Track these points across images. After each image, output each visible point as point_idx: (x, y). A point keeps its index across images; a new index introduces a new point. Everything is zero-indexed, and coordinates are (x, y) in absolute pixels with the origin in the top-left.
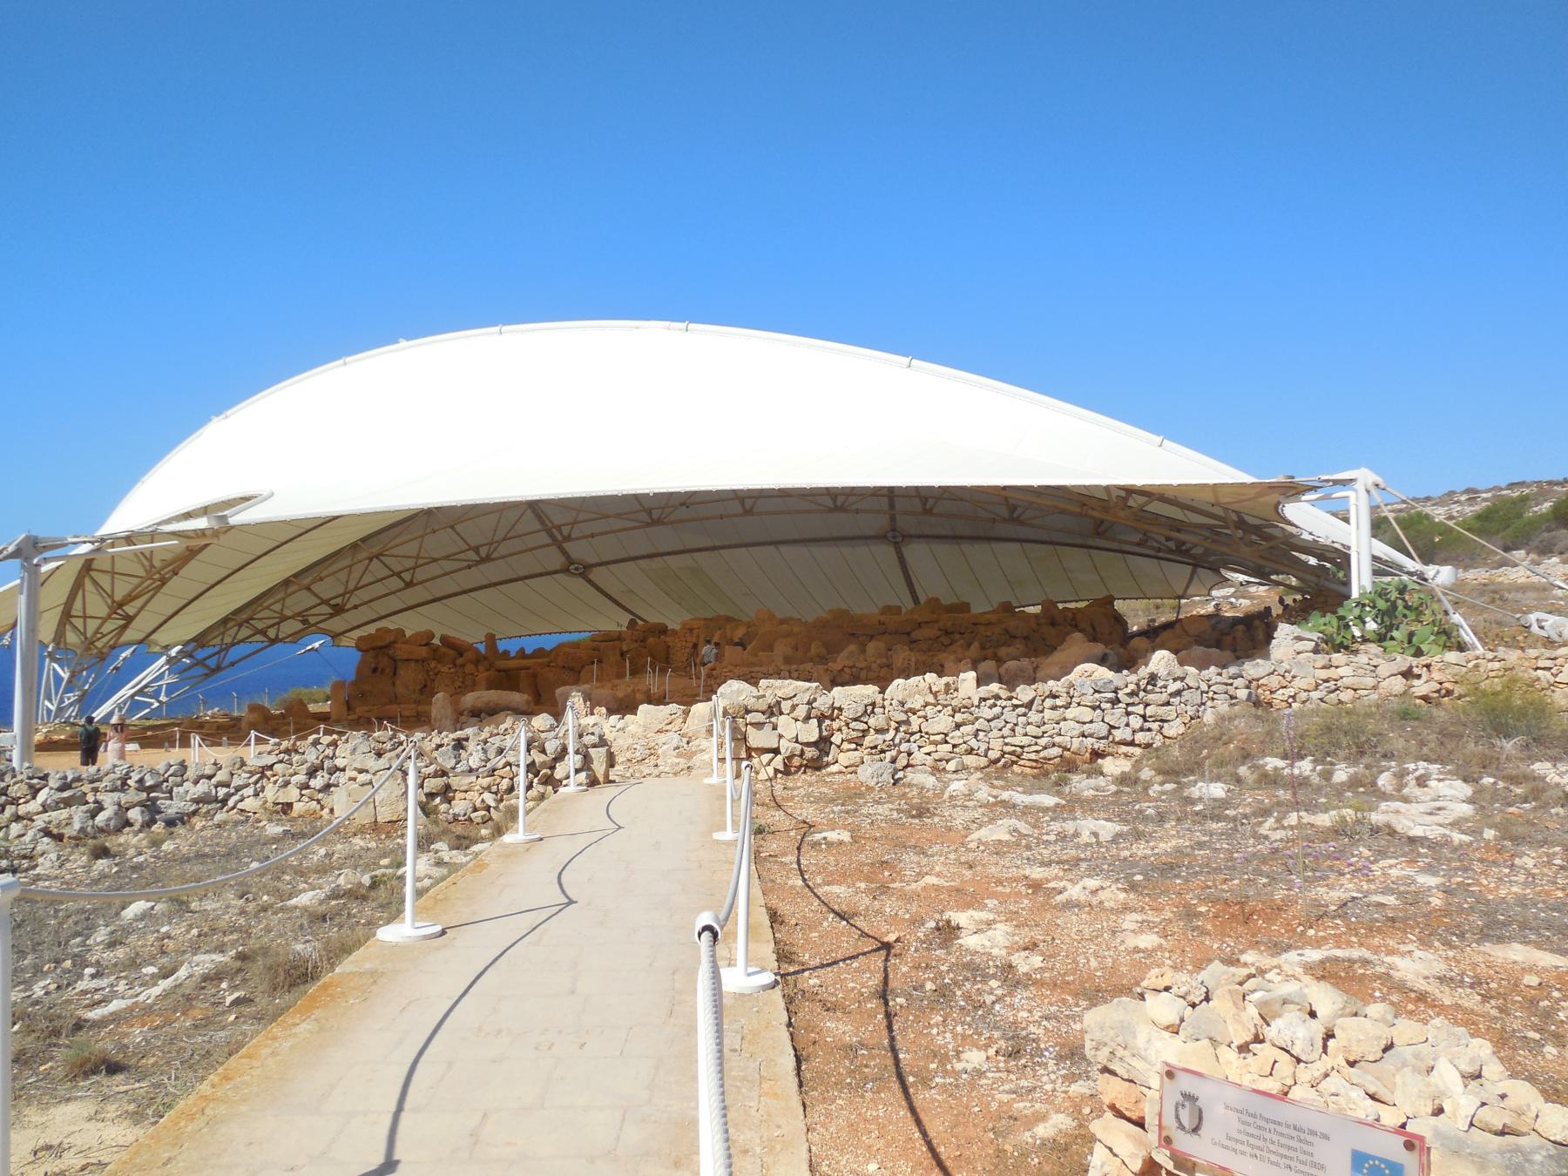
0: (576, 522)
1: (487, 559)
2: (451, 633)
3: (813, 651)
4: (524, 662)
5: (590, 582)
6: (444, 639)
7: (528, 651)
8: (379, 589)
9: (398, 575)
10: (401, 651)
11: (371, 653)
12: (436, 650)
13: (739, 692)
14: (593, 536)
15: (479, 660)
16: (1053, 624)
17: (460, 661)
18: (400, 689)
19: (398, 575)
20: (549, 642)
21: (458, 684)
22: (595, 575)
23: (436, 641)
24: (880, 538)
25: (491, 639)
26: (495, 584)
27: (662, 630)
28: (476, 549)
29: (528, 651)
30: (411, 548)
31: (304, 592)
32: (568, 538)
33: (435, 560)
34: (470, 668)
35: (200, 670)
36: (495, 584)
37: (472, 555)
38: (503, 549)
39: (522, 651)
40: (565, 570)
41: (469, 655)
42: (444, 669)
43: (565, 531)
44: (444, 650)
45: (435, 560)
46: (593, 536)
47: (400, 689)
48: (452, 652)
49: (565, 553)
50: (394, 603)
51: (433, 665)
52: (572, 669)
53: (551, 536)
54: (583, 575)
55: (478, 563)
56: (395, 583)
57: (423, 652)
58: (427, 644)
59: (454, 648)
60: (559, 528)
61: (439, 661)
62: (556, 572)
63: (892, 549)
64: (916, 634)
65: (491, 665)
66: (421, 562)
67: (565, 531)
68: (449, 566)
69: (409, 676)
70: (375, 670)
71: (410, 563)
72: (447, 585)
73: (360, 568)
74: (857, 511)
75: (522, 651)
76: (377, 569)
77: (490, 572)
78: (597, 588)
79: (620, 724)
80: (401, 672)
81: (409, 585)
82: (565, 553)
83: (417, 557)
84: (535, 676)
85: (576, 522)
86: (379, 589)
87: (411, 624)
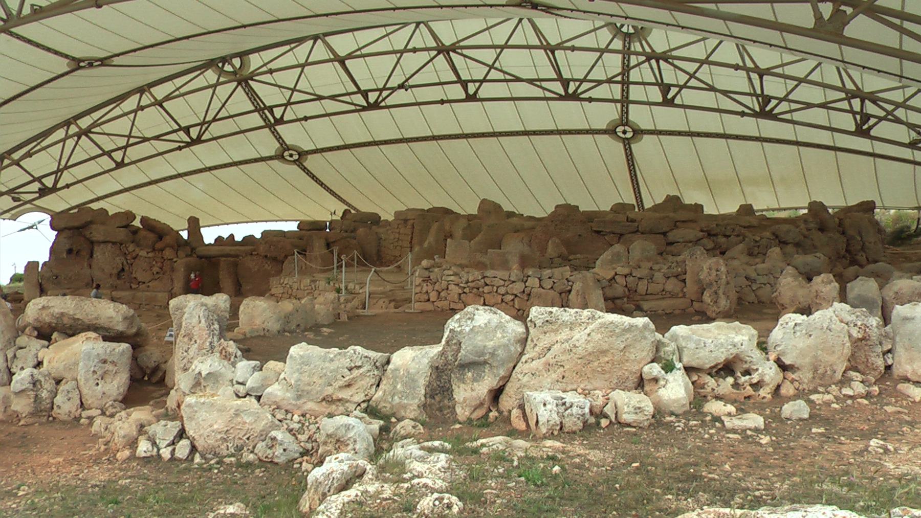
0: (289, 103)
1: (198, 141)
2: (154, 215)
3: (551, 250)
4: (227, 249)
5: (304, 169)
6: (144, 220)
7: (238, 238)
8: (92, 168)
9: (109, 154)
11: (64, 235)
12: (136, 231)
13: (487, 330)
14: (306, 119)
15: (180, 244)
16: (822, 229)
19: (109, 154)
20: (256, 230)
21: (156, 269)
22: (311, 162)
23: (137, 223)
24: (611, 131)
25: (194, 225)
26: (210, 169)
27: (374, 219)
28: (187, 130)
29: (238, 238)
30: (122, 127)
31: (15, 167)
32: (280, 121)
33: (145, 140)
34: (168, 253)
36: (210, 169)
37: (182, 136)
38: (216, 129)
39: (232, 236)
40: (280, 157)
41: (168, 239)
42: (143, 253)
43: (278, 112)
44: (143, 233)
45: (145, 140)
46: (306, 119)
47: (97, 274)
48: (151, 236)
49: (279, 138)
50: (107, 185)
51: (131, 248)
52: (275, 259)
53: (265, 119)
54: (299, 163)
55: (188, 145)
57: (122, 235)
58: (126, 227)
59: (156, 233)
60: (271, 109)
62: (271, 158)
63: (621, 145)
64: (671, 236)
65: (193, 249)
66: (132, 141)
67: (278, 112)
68: (162, 146)
70: (70, 251)
71: (122, 142)
72: (159, 169)
73: (70, 143)
74: (590, 100)
75: (232, 236)
76: (86, 147)
77: (206, 155)
78: (313, 177)
79: (253, 381)
80: (98, 254)
81: (120, 165)
82: (279, 138)
83: (129, 136)
84: (236, 265)
85: (289, 103)
86: (92, 168)
87: (113, 206)
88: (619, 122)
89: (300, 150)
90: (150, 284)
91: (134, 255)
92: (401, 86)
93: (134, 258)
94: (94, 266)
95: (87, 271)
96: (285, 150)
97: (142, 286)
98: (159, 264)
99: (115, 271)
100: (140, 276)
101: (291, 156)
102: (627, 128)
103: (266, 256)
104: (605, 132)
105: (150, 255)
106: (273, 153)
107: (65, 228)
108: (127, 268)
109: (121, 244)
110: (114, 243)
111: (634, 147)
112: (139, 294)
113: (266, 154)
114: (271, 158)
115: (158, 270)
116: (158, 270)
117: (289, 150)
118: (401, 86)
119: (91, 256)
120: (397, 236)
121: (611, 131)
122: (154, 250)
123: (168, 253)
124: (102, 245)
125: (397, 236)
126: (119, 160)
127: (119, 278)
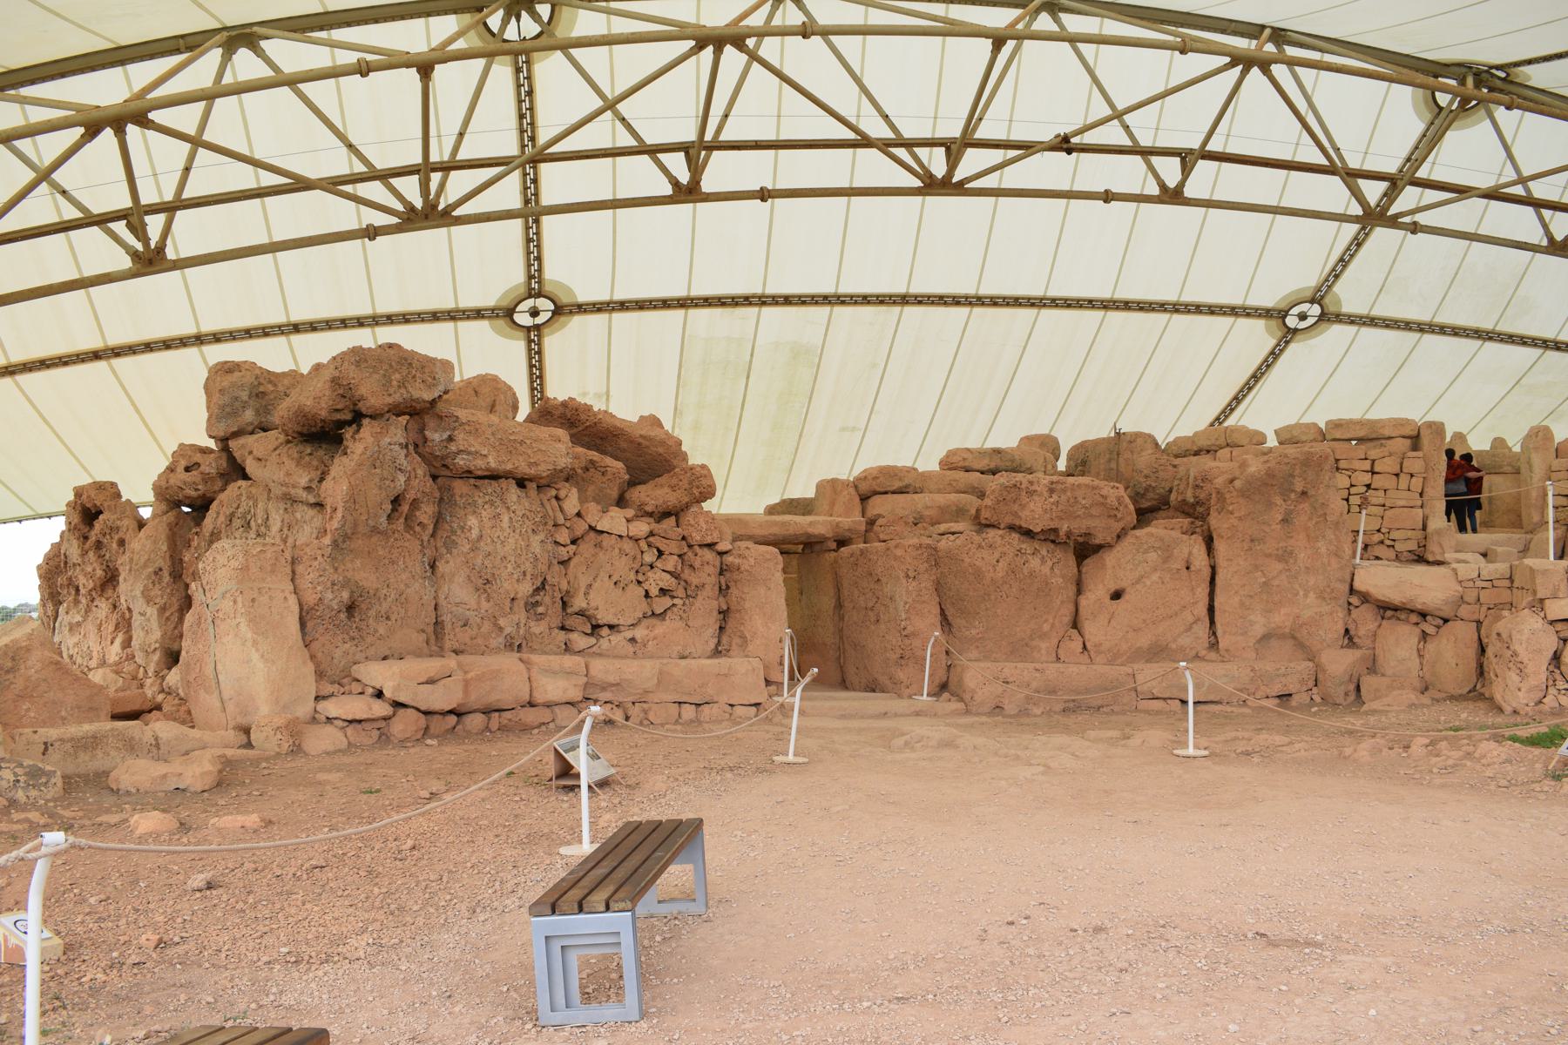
18: (458, 592)
21: (657, 579)
42: (614, 521)
47: (458, 592)
56: (100, 251)
62: (478, 314)
88: (1309, 294)
90: (639, 633)
91: (581, 527)
92: (1064, 144)
95: (420, 590)
96: (531, 294)
97: (609, 641)
98: (671, 563)
99: (526, 588)
100: (603, 601)
101: (534, 313)
102: (1316, 310)
103: (1050, 537)
104: (1266, 313)
106: (489, 300)
110: (521, 483)
111: (1292, 346)
113: (468, 302)
114: (478, 314)
117: (539, 295)
118: (1064, 144)
120: (1367, 478)
121: (1276, 315)
125: (1367, 478)
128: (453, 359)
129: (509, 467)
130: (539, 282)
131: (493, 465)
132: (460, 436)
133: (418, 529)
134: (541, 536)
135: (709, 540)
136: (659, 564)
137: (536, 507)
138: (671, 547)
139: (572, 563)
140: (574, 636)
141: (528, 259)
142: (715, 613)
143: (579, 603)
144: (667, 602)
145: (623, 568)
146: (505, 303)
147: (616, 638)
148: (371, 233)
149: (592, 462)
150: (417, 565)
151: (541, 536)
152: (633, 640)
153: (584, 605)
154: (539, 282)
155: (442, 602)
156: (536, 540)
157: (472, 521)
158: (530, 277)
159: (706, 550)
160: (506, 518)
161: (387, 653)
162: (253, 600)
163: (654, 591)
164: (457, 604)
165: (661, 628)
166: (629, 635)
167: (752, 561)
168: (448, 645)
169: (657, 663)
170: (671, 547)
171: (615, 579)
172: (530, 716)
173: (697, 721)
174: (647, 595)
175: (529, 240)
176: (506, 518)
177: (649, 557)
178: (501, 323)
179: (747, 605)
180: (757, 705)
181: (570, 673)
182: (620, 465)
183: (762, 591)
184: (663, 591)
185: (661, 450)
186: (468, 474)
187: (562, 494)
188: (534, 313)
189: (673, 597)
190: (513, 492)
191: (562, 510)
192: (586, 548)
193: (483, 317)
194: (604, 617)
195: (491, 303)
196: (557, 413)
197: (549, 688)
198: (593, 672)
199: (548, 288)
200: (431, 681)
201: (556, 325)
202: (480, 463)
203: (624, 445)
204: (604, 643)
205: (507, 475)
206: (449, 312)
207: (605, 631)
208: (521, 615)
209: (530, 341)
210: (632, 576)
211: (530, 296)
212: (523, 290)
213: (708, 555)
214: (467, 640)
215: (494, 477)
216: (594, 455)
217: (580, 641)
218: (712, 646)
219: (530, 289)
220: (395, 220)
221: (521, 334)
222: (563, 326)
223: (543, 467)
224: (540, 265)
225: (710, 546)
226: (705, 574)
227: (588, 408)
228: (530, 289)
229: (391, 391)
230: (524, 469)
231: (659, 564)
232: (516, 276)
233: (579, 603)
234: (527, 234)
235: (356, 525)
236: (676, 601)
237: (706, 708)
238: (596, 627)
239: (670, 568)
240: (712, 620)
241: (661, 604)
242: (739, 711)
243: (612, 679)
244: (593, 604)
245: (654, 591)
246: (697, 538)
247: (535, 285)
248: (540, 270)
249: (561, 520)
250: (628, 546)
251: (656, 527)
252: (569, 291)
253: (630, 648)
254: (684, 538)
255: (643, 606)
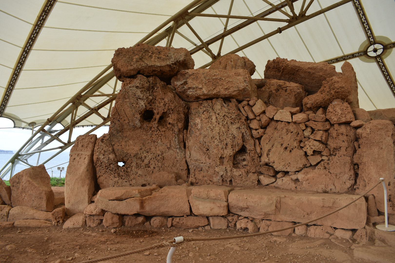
10: (196, 87)
17: (310, 100)
18: (195, 155)
21: (311, 146)
23: (259, 74)
35: (56, 144)
42: (283, 115)
47: (195, 155)
48: (293, 85)
51: (259, 107)
61: (267, 103)
62: (353, 56)
69: (212, 128)
70: (147, 115)
80: (197, 121)
89: (387, 43)
90: (300, 176)
91: (264, 119)
93: (264, 127)
94: (190, 143)
96: (371, 44)
98: (319, 135)
99: (229, 152)
100: (277, 158)
101: (375, 50)
105: (300, 117)
106: (356, 50)
107: (139, 72)
108: (249, 146)
109: (240, 102)
110: (227, 99)
112: (292, 200)
114: (353, 56)
115: (318, 146)
116: (318, 146)
117: (375, 43)
119: (186, 126)
122: (301, 111)
123: (338, 111)
124: (205, 104)
126: (216, 54)
127: (235, 165)
128: (244, 56)
129: (215, 92)
130: (373, 38)
131: (206, 92)
132: (189, 81)
133: (168, 126)
134: (237, 125)
135: (343, 120)
136: (312, 137)
137: (233, 110)
138: (319, 126)
139: (262, 139)
140: (261, 177)
141: (366, 30)
142: (348, 165)
143: (264, 159)
144: (318, 158)
145: (289, 140)
146: (362, 49)
147: (286, 179)
148: (280, 30)
149: (280, 86)
150: (175, 142)
151: (237, 125)
152: (297, 180)
153: (267, 160)
154: (373, 38)
155: (188, 160)
156: (233, 129)
157: (198, 121)
158: (369, 37)
159: (343, 127)
160: (214, 118)
161: (144, 183)
162: (74, 159)
163: (310, 152)
164: (196, 160)
165: (312, 174)
166: (294, 177)
167: (368, 130)
168: (190, 180)
169: (274, 196)
170: (319, 126)
171: (284, 146)
172: (190, 221)
173: (304, 237)
174: (306, 154)
175: (363, 23)
176: (214, 118)
177: (307, 133)
178: (363, 57)
179: (365, 160)
180: (354, 231)
181: (214, 200)
182: (297, 85)
183: (376, 150)
184: (315, 152)
185: (321, 74)
186: (197, 99)
187: (251, 103)
188: (375, 50)
189: (322, 156)
190: (218, 105)
191: (252, 111)
192: (269, 130)
193: (356, 57)
194: (278, 167)
195: (356, 50)
196: (272, 66)
197: (201, 207)
198: (229, 201)
199: (377, 40)
200: (119, 199)
201: (387, 54)
202: (199, 92)
203: (303, 75)
204: (279, 182)
205: (216, 97)
206: (342, 57)
207: (279, 175)
208: (228, 165)
209: (378, 62)
210: (295, 144)
211: (371, 45)
212: (367, 43)
213: (343, 129)
214: (200, 177)
215: (210, 98)
216: (281, 82)
217: (265, 180)
218: (348, 184)
219: (370, 42)
220: (286, 24)
221: (373, 60)
222: (390, 53)
223: (231, 90)
224: (371, 31)
225: (348, 123)
226: (340, 139)
227: (284, 60)
228: (370, 42)
229: (132, 63)
230: (224, 92)
231: (312, 137)
232: (364, 38)
233: (264, 159)
234: (362, 21)
235: (123, 126)
236: (324, 158)
237: (312, 229)
238: (277, 173)
239: (318, 138)
240: (347, 170)
241: (314, 160)
242: (338, 233)
243: (241, 204)
244: (271, 160)
245: (310, 152)
246: (334, 119)
247: (371, 40)
248: (372, 33)
249: (251, 116)
250: (291, 127)
251: (311, 115)
252: (387, 39)
253: (293, 185)
254: (327, 120)
255: (304, 161)
